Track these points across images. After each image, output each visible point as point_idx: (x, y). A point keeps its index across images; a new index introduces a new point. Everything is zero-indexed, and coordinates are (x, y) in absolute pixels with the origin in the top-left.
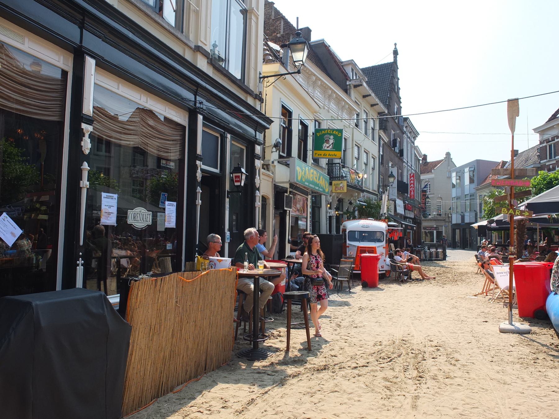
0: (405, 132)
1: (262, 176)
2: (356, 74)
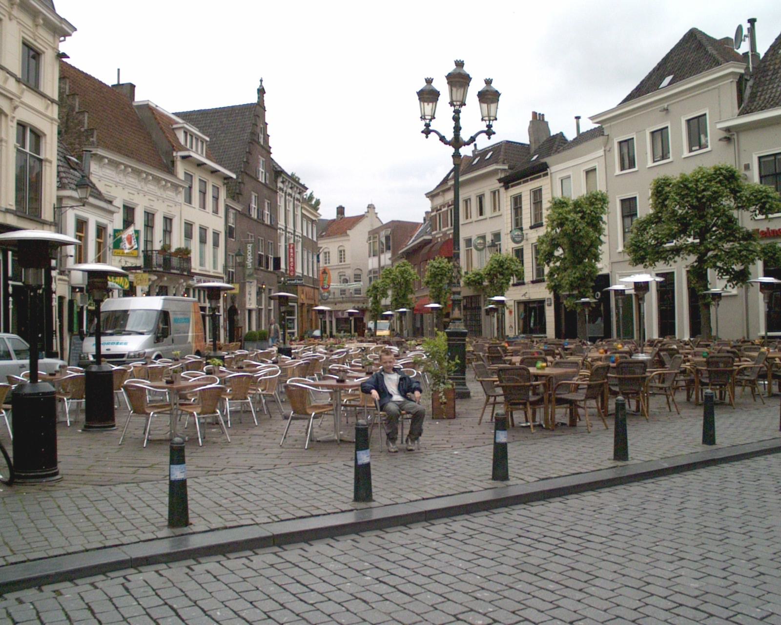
1: (57, 282)
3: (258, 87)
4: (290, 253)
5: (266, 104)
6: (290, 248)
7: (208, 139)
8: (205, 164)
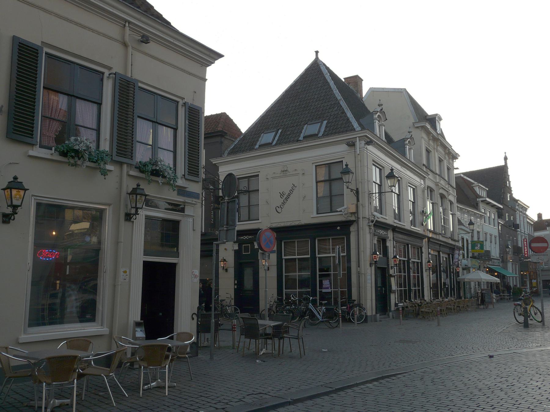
0: (517, 209)
2: (481, 189)
4: (524, 244)
5: (509, 165)
6: (524, 241)
7: (487, 189)
8: (491, 203)
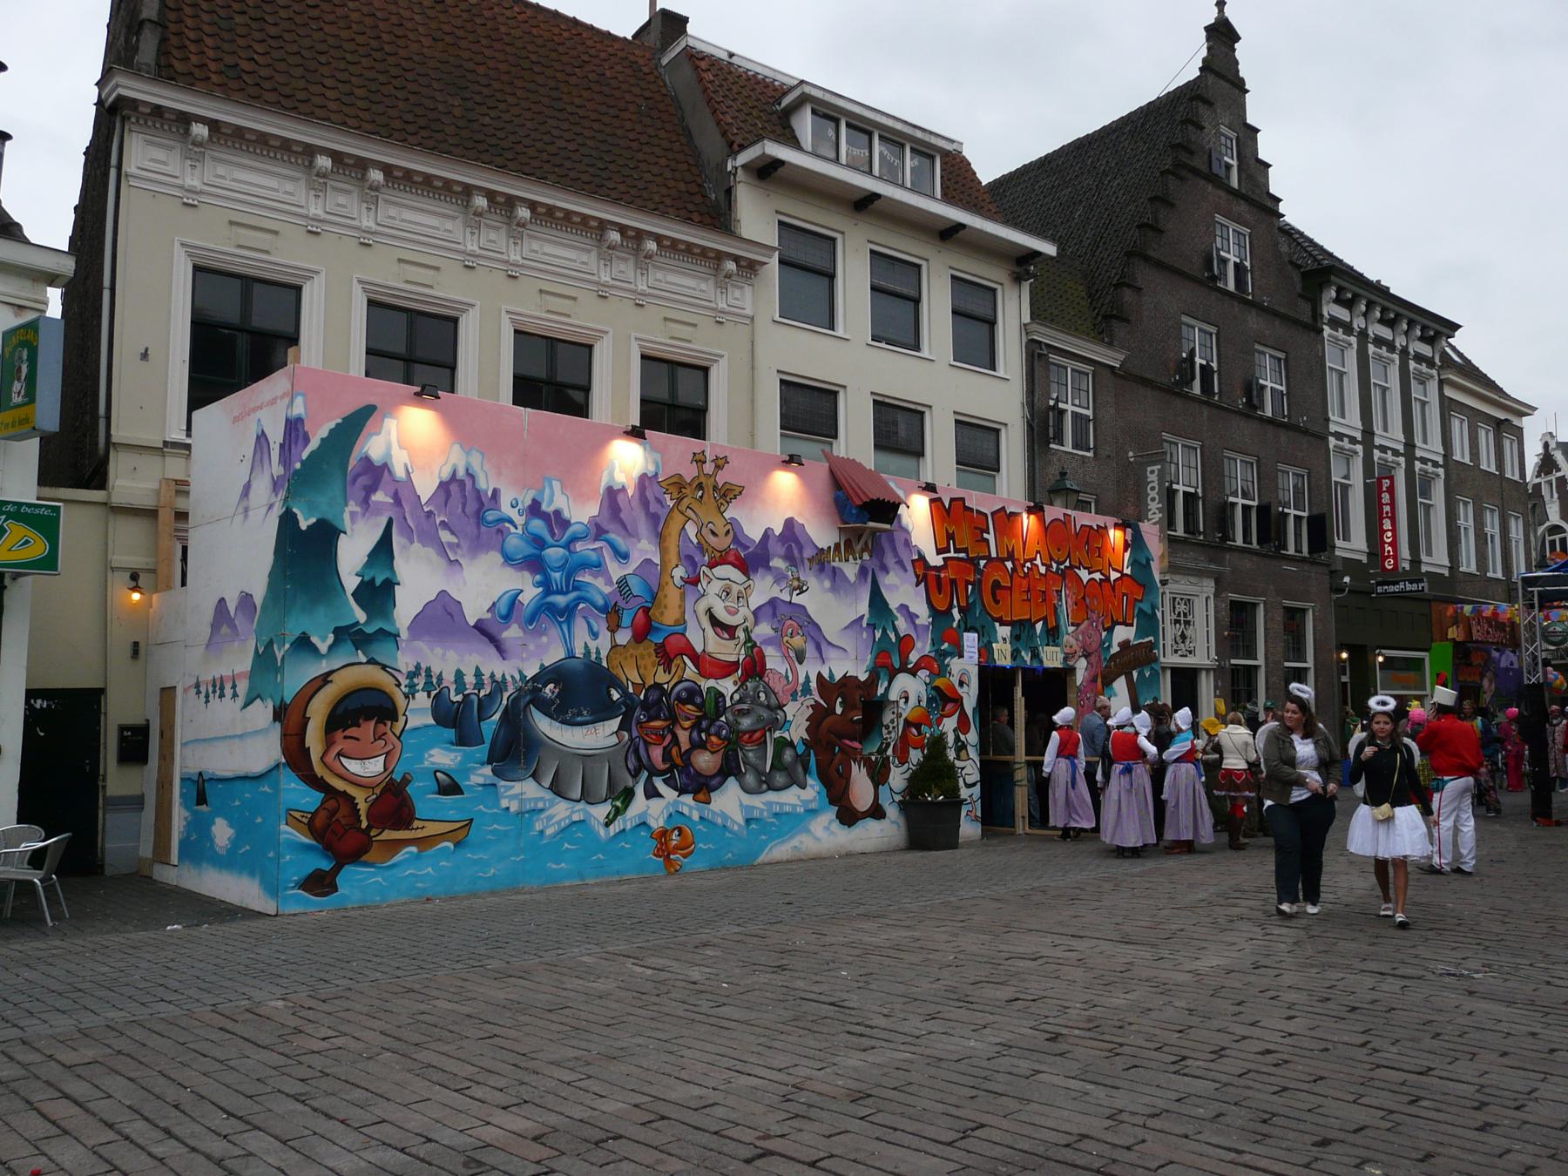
3: (1211, 16)
